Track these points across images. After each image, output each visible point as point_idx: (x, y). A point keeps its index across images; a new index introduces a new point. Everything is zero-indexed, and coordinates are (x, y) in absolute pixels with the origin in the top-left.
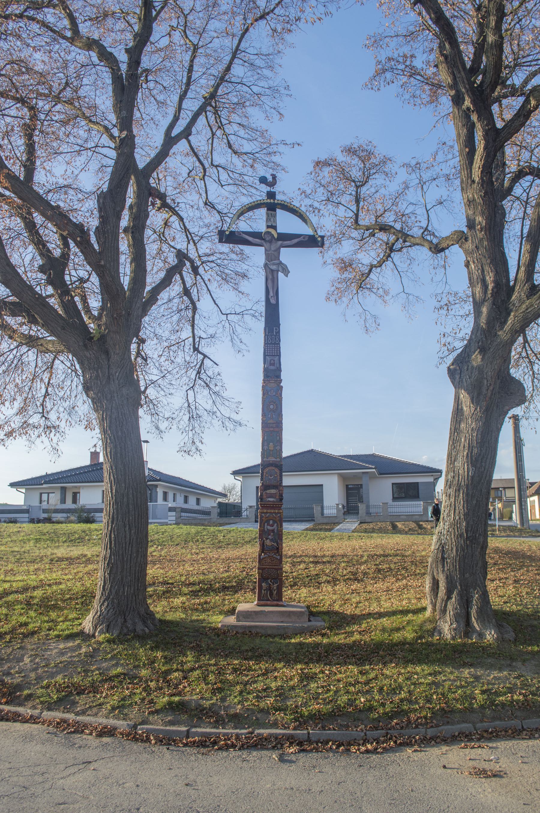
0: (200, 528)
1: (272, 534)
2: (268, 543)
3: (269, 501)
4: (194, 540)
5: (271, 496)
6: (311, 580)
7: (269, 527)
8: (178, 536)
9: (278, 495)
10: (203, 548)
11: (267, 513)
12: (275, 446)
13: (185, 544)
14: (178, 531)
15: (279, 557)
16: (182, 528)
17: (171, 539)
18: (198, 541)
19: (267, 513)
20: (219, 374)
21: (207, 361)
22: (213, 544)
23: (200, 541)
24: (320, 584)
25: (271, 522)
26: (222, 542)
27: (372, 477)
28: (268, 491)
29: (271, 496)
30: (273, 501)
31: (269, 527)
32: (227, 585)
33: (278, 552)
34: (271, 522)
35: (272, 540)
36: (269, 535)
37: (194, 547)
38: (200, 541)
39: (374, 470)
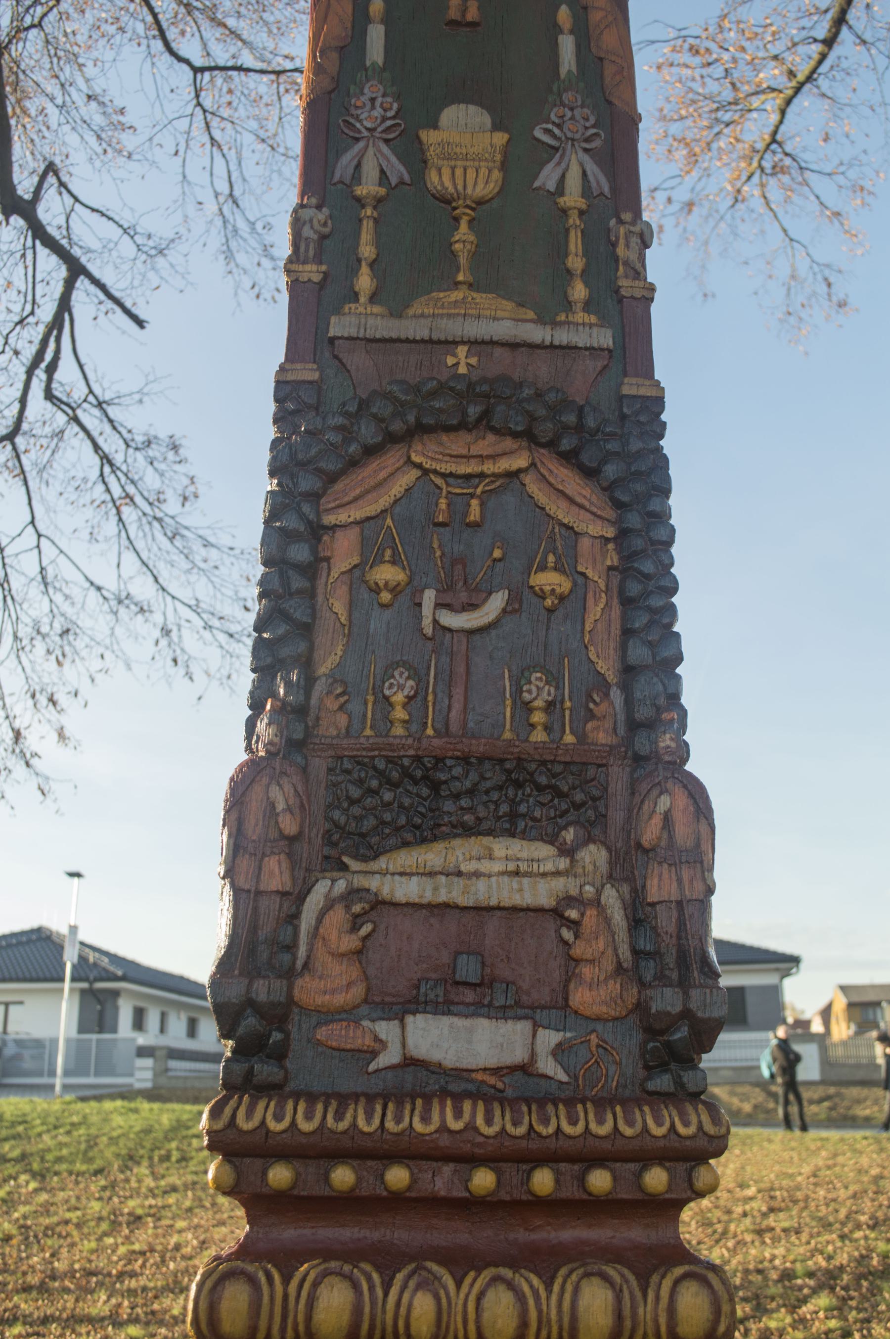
3: (423, 1081)
5: (471, 964)
8: (113, 1141)
9: (605, 939)
10: (174, 1189)
12: (521, 160)
13: (123, 1169)
14: (118, 1120)
16: (136, 1111)
17: (90, 1147)
18: (167, 1158)
20: (175, 448)
21: (84, 297)
23: (175, 1156)
28: (405, 877)
29: (471, 964)
30: (513, 1086)
37: (150, 1182)
38: (175, 1156)
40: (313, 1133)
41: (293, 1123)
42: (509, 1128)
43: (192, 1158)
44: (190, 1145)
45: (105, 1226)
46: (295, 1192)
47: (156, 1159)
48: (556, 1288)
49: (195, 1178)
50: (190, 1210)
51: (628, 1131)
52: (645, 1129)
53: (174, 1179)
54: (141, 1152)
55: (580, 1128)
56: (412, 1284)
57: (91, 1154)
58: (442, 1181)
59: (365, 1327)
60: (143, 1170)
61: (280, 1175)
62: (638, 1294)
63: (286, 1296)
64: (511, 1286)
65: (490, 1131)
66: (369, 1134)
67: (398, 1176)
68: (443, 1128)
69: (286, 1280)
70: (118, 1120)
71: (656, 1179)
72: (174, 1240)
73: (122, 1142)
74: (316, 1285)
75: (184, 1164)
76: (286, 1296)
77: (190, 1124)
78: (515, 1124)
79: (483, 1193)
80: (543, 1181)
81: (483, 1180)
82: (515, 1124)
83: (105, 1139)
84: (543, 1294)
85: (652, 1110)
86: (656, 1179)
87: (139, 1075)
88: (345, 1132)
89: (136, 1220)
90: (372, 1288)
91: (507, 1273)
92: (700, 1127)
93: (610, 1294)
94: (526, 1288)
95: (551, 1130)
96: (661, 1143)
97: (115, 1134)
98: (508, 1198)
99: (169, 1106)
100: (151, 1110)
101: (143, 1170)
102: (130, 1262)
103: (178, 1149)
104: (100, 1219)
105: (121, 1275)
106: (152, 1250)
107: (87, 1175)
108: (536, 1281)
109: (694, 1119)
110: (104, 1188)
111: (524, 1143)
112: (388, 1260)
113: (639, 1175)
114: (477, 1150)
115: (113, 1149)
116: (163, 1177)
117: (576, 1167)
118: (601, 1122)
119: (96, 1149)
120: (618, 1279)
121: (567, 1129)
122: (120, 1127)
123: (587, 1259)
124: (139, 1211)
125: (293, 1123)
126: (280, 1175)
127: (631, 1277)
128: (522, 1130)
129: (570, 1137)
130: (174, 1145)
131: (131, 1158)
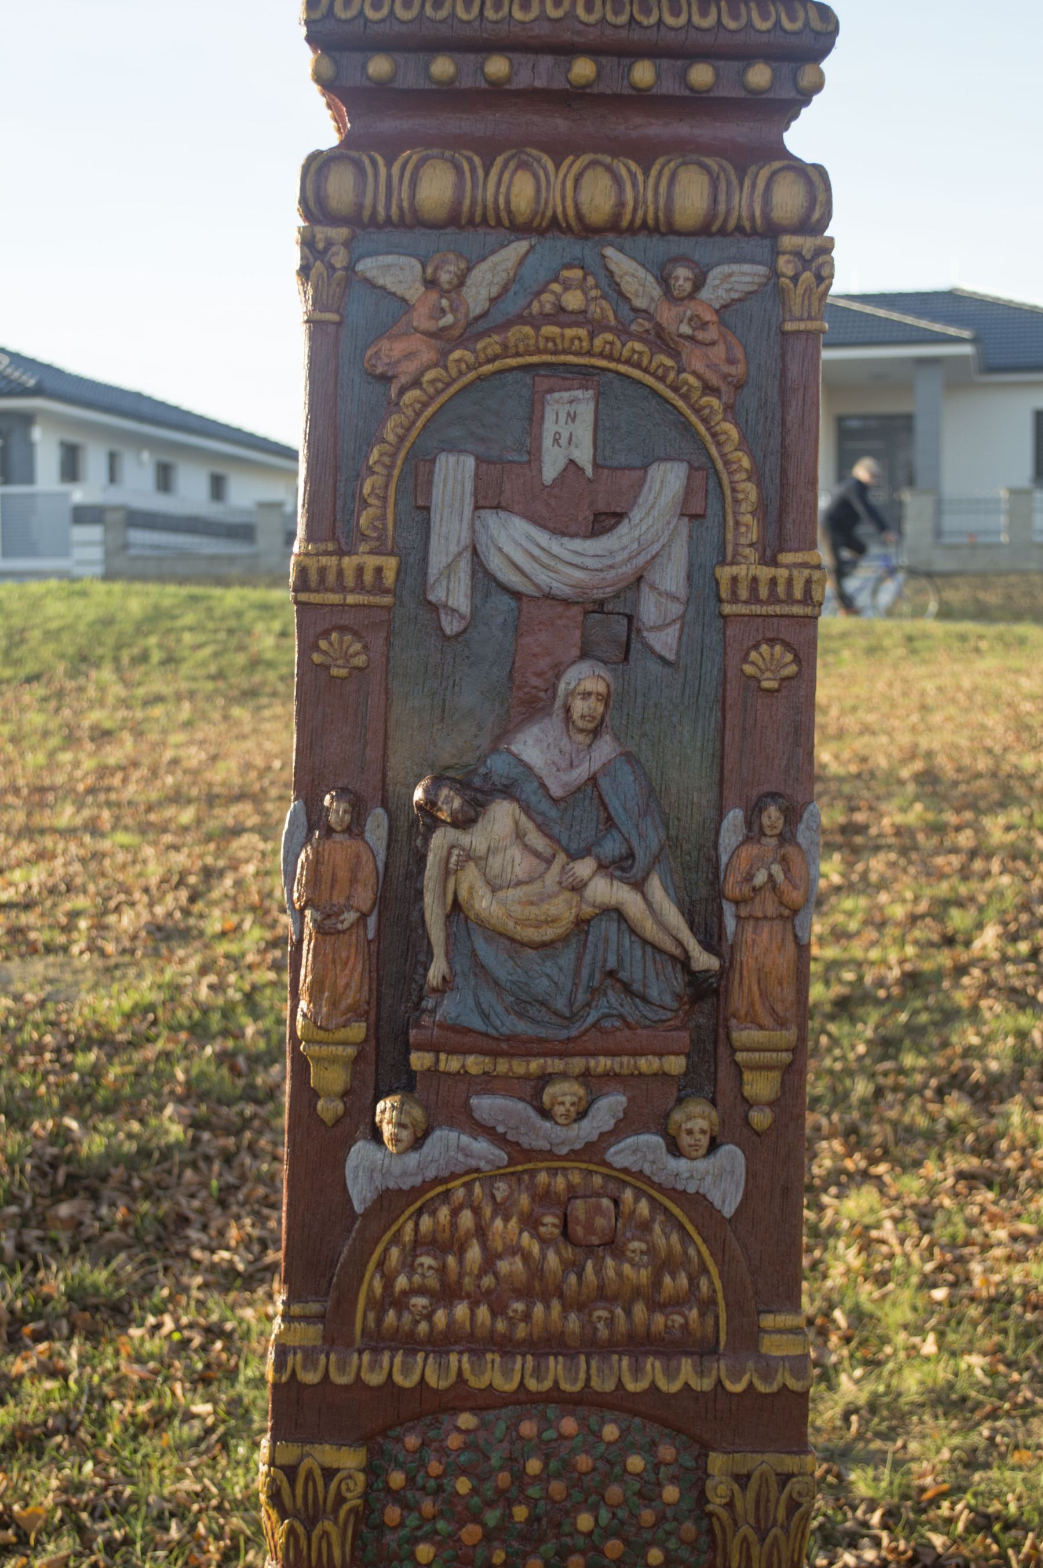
0: (171, 594)
1: (585, 681)
2: (501, 872)
4: (125, 657)
6: (887, 1046)
7: (518, 545)
8: (51, 636)
10: (159, 699)
11: (471, 224)
13: (73, 674)
15: (722, 1179)
18: (144, 657)
19: (471, 224)
22: (220, 675)
23: (156, 656)
24: (988, 1095)
25: (568, 432)
26: (270, 665)
27: (956, 378)
31: (518, 545)
32: (93, 1145)
33: (710, 1064)
34: (568, 432)
35: (578, 821)
36: (534, 705)
37: (117, 690)
38: (156, 656)
39: (967, 350)
40: (412, 21)
41: (392, 12)
42: (610, 17)
43: (183, 659)
44: (179, 641)
45: (54, 742)
46: (397, 85)
47: (125, 660)
48: (654, 172)
49: (193, 686)
50: (188, 725)
51: (732, 25)
52: (749, 24)
53: (157, 685)
54: (100, 651)
55: (682, 20)
56: (512, 165)
57: (16, 654)
58: (540, 72)
59: (467, 202)
60: (106, 674)
61: (379, 66)
62: (735, 182)
63: (389, 176)
64: (609, 169)
65: (591, 19)
66: (468, 22)
67: (497, 66)
68: (543, 16)
69: (389, 165)
70: (54, 608)
71: (759, 75)
72: (168, 754)
73: (65, 637)
74: (417, 168)
75: (173, 666)
76: (389, 176)
77: (177, 611)
78: (616, 13)
79: (583, 81)
80: (643, 73)
81: (583, 69)
82: (616, 13)
83: (36, 634)
84: (640, 178)
85: (758, 5)
86: (759, 75)
87: (79, 553)
88: (443, 21)
89: (103, 735)
90: (473, 170)
91: (607, 159)
92: (807, 23)
93: (706, 179)
94: (624, 172)
95: (653, 20)
96: (764, 39)
97: (54, 625)
98: (609, 91)
99: (138, 586)
100: (109, 593)
101: (106, 674)
102: (101, 777)
103: (160, 646)
104: (46, 734)
105: (91, 791)
106: (135, 764)
107: (15, 683)
108: (633, 166)
109: (801, 15)
110: (45, 699)
111: (624, 33)
112: (488, 150)
113: (743, 73)
114: (576, 39)
115: (52, 647)
116: (140, 684)
117: (679, 63)
118: (704, 14)
119: (24, 648)
120: (715, 168)
121: (669, 20)
122: (61, 616)
123: (686, 150)
124: (108, 725)
125: (392, 12)
126: (379, 66)
127: (729, 167)
128: (623, 19)
129: (671, 29)
130: (152, 640)
131: (84, 659)
